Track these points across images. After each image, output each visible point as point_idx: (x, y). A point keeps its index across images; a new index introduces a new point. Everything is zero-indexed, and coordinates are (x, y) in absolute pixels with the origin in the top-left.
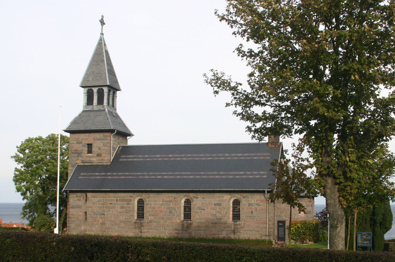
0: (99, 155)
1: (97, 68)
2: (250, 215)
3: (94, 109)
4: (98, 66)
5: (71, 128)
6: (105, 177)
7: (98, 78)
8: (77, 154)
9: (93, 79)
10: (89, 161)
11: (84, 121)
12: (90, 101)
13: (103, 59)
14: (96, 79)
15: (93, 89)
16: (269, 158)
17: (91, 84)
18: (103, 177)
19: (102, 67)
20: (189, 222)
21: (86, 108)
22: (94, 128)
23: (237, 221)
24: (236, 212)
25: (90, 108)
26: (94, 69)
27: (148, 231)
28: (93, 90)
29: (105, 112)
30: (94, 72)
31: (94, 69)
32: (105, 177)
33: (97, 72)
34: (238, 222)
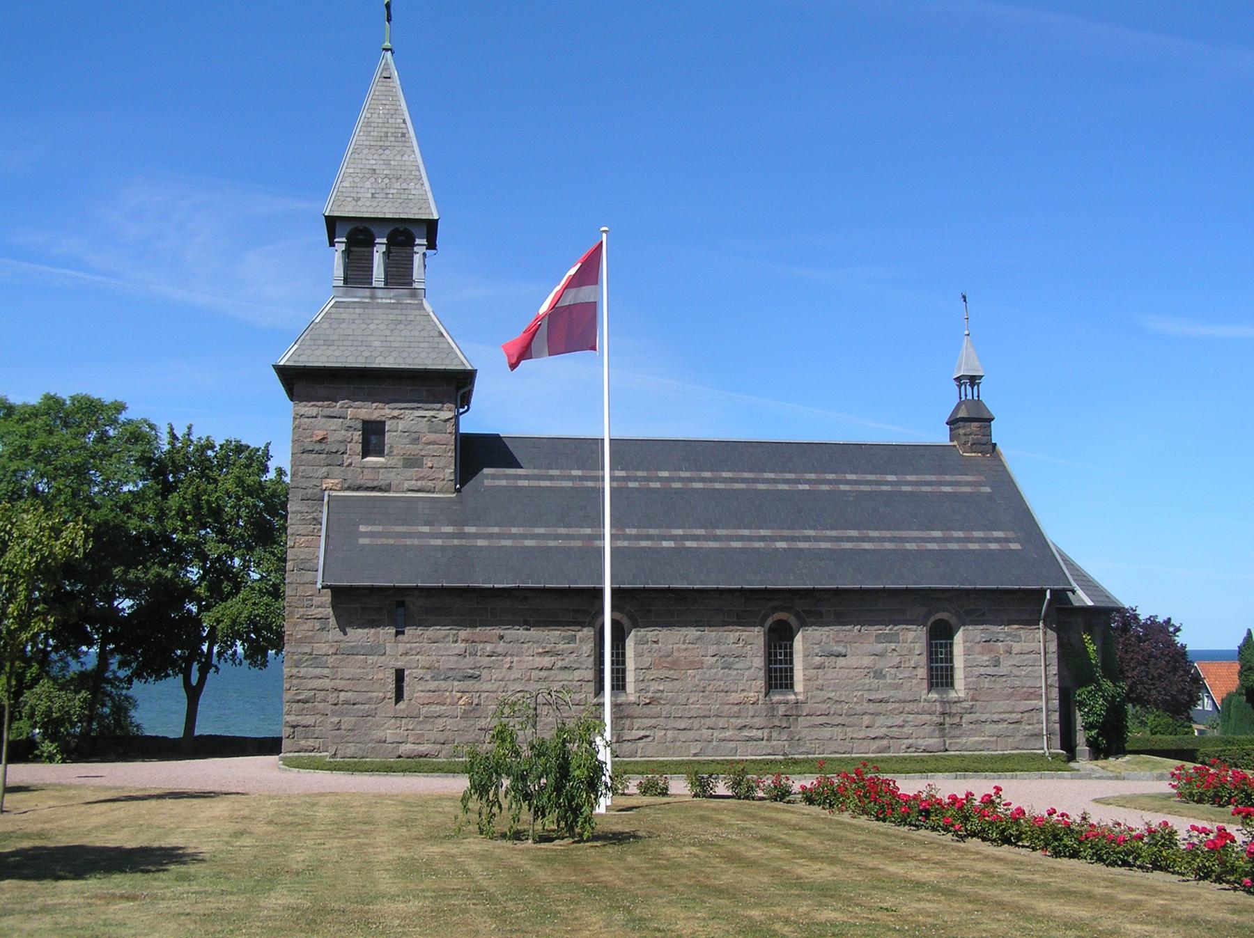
0: (412, 462)
1: (382, 157)
2: (990, 670)
3: (380, 301)
4: (387, 152)
5: (301, 359)
6: (464, 542)
7: (395, 191)
8: (323, 456)
9: (377, 196)
10: (375, 483)
11: (350, 338)
12: (356, 273)
13: (405, 131)
14: (387, 194)
15: (374, 229)
16: (987, 489)
17: (370, 209)
18: (456, 542)
19: (405, 158)
20: (792, 697)
21: (346, 295)
22: (399, 364)
23: (947, 693)
24: (942, 662)
25: (361, 295)
26: (374, 162)
27: (642, 733)
28: (375, 232)
29: (422, 312)
30: (374, 170)
31: (374, 162)
32: (464, 542)
33: (385, 172)
34: (953, 695)
